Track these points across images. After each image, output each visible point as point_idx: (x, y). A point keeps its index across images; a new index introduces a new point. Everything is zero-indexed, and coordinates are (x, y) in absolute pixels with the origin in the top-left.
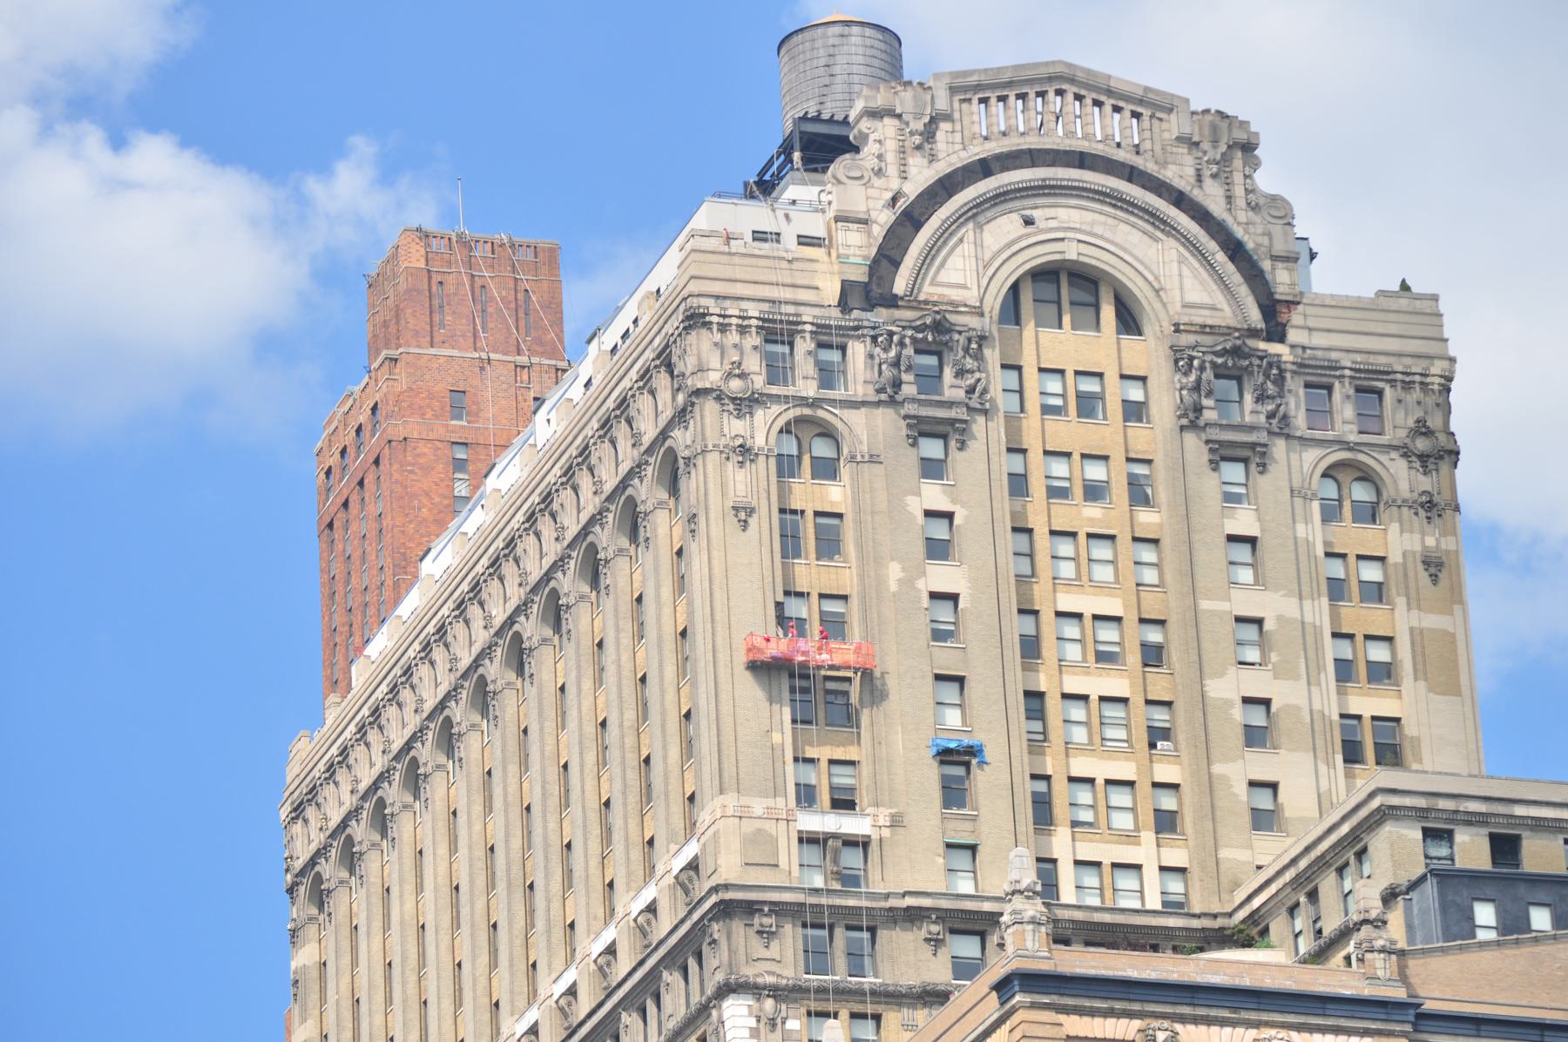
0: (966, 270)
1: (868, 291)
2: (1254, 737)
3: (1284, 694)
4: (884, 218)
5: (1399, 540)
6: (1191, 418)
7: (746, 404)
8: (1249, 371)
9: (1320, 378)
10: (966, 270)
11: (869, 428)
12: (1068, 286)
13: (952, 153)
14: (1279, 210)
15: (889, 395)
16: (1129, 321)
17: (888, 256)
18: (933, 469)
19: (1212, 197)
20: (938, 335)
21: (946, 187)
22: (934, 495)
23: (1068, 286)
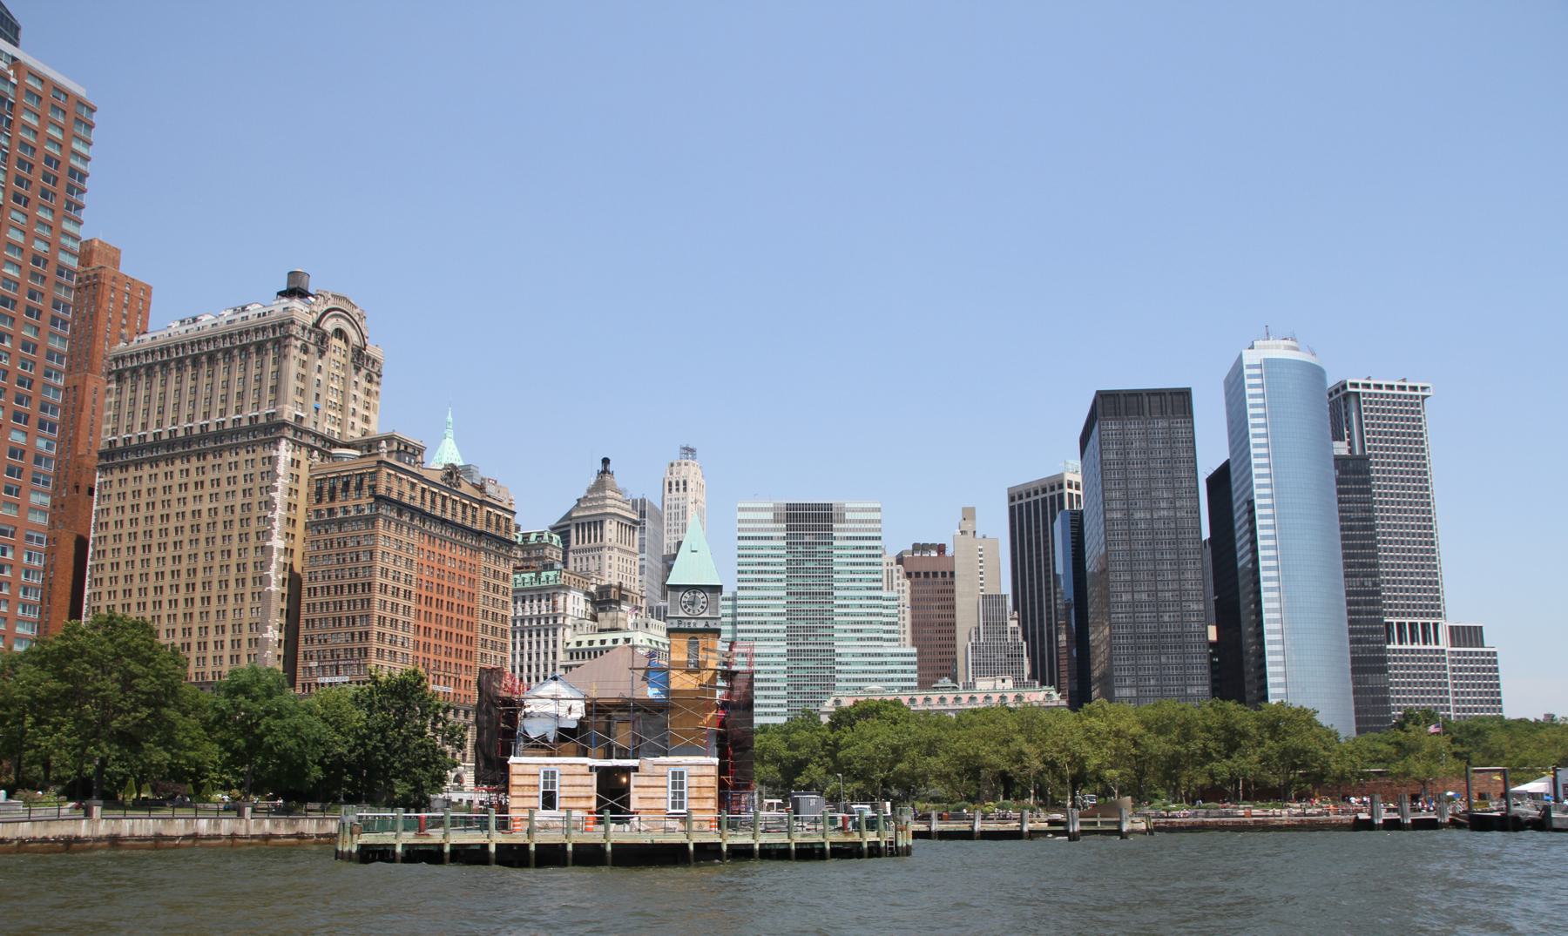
0: (329, 325)
1: (316, 325)
2: (354, 414)
8: (360, 357)
9: (368, 358)
10: (329, 325)
11: (312, 348)
12: (339, 333)
13: (330, 306)
15: (315, 344)
16: (346, 341)
17: (319, 320)
20: (324, 334)
21: (329, 311)
22: (319, 362)
23: (339, 333)
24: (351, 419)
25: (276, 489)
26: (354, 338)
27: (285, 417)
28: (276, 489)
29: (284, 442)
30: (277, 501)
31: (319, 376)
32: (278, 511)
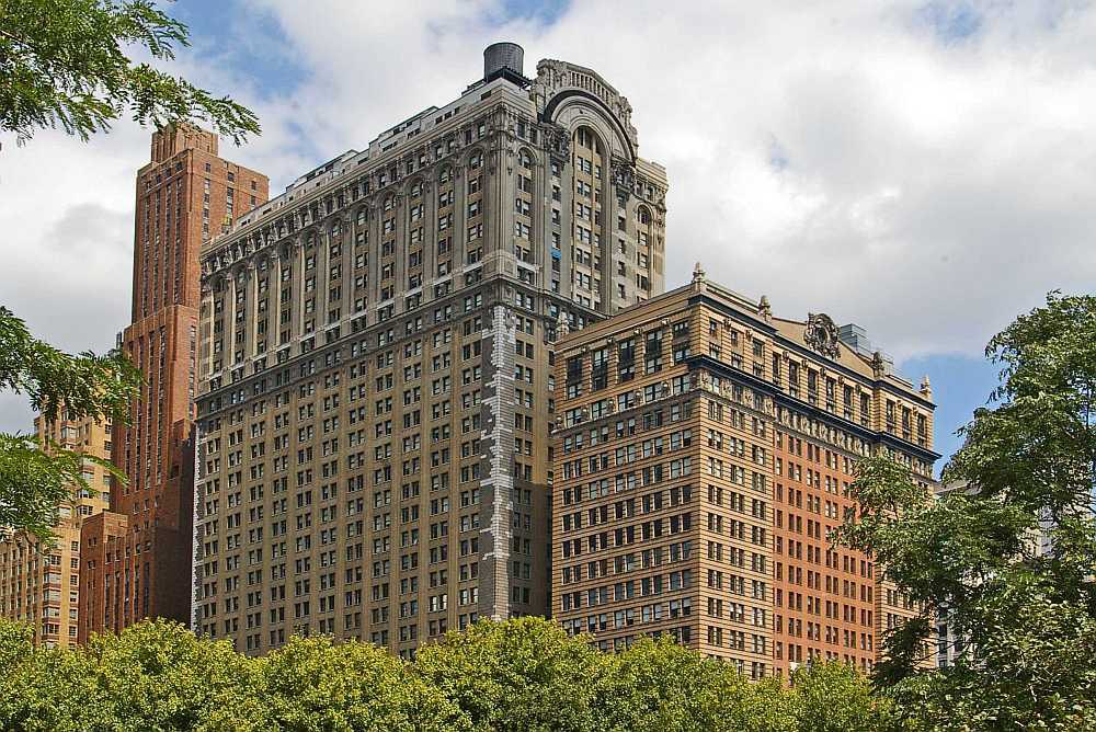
0: (568, 118)
1: (545, 116)
2: (622, 272)
3: (628, 263)
4: (549, 98)
5: (654, 231)
6: (613, 181)
7: (511, 138)
14: (635, 132)
15: (546, 148)
17: (550, 109)
18: (557, 174)
19: (622, 121)
22: (555, 181)
23: (587, 134)
24: (618, 280)
25: (492, 392)
26: (615, 145)
27: (501, 269)
28: (492, 392)
29: (500, 311)
30: (496, 411)
31: (555, 205)
32: (499, 427)
